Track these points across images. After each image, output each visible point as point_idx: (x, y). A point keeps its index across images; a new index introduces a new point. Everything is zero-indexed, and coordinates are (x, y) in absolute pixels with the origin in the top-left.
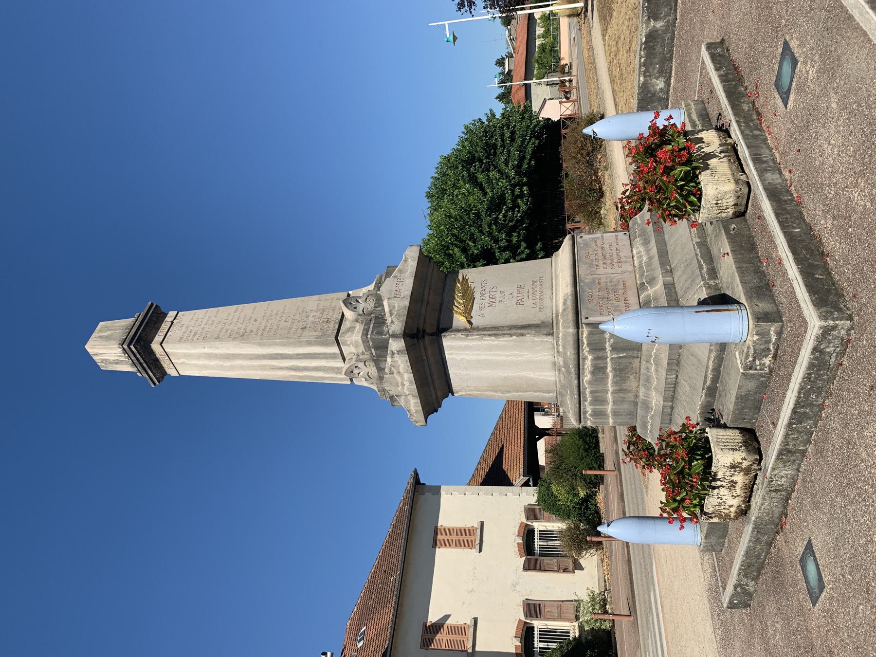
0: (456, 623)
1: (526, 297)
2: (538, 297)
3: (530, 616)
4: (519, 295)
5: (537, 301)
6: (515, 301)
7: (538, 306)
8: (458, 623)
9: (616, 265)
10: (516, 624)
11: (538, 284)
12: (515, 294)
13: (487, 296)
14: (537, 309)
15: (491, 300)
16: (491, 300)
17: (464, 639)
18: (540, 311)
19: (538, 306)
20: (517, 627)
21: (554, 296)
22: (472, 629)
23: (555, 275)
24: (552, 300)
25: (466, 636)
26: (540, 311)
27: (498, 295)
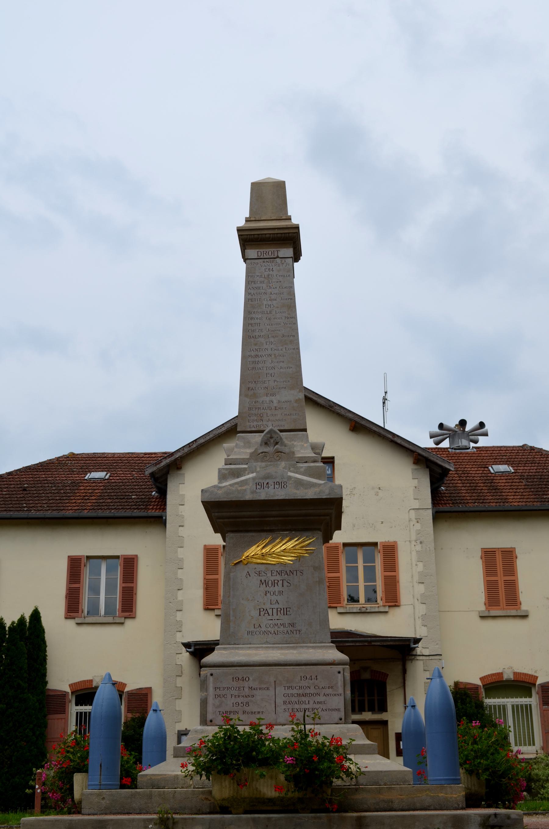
0: (520, 591)
1: (270, 617)
2: (269, 629)
3: (543, 691)
4: (275, 611)
5: (264, 629)
6: (268, 606)
7: (255, 630)
8: (520, 593)
9: (290, 706)
10: (530, 673)
11: (291, 628)
12: (276, 606)
13: (278, 578)
14: (252, 629)
15: (270, 583)
16: (270, 583)
17: (501, 605)
18: (248, 633)
19: (255, 630)
20: (526, 675)
21: (269, 646)
22: (513, 613)
23: (297, 647)
24: (264, 643)
25: (505, 607)
26: (248, 633)
27: (277, 589)
